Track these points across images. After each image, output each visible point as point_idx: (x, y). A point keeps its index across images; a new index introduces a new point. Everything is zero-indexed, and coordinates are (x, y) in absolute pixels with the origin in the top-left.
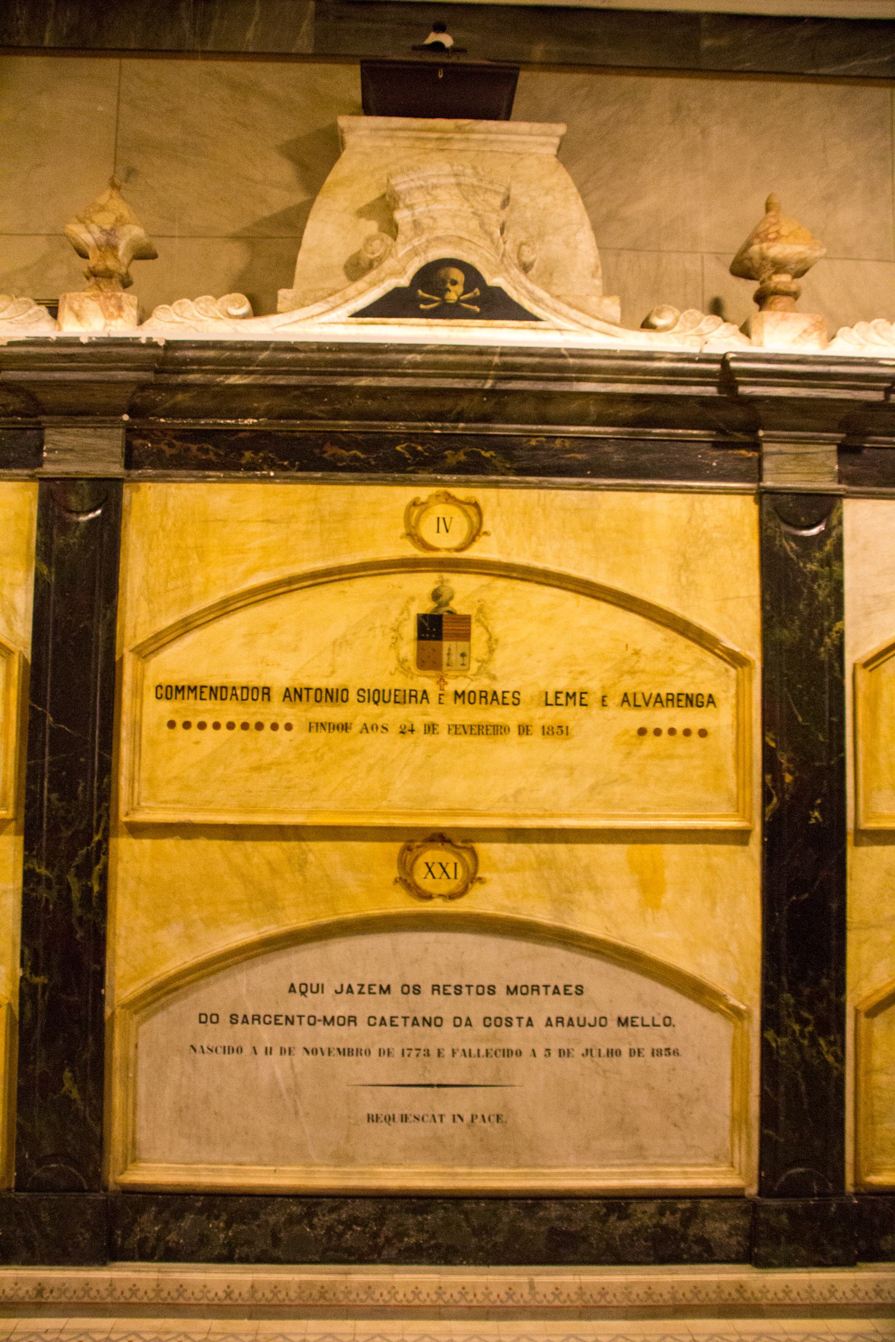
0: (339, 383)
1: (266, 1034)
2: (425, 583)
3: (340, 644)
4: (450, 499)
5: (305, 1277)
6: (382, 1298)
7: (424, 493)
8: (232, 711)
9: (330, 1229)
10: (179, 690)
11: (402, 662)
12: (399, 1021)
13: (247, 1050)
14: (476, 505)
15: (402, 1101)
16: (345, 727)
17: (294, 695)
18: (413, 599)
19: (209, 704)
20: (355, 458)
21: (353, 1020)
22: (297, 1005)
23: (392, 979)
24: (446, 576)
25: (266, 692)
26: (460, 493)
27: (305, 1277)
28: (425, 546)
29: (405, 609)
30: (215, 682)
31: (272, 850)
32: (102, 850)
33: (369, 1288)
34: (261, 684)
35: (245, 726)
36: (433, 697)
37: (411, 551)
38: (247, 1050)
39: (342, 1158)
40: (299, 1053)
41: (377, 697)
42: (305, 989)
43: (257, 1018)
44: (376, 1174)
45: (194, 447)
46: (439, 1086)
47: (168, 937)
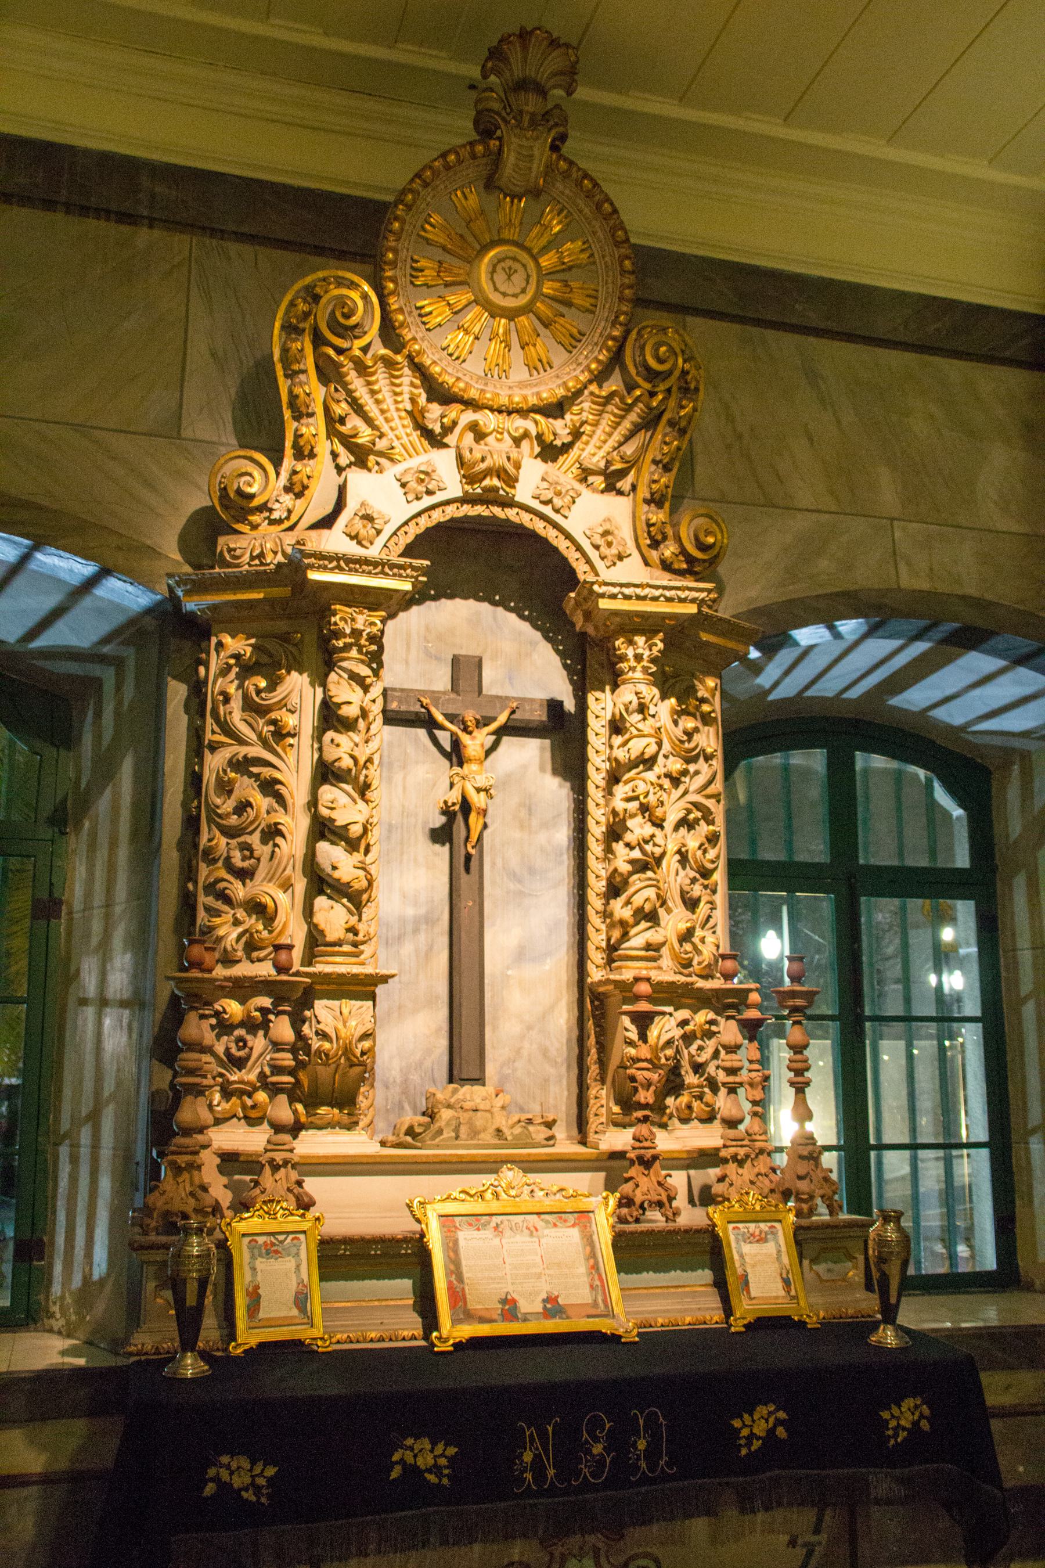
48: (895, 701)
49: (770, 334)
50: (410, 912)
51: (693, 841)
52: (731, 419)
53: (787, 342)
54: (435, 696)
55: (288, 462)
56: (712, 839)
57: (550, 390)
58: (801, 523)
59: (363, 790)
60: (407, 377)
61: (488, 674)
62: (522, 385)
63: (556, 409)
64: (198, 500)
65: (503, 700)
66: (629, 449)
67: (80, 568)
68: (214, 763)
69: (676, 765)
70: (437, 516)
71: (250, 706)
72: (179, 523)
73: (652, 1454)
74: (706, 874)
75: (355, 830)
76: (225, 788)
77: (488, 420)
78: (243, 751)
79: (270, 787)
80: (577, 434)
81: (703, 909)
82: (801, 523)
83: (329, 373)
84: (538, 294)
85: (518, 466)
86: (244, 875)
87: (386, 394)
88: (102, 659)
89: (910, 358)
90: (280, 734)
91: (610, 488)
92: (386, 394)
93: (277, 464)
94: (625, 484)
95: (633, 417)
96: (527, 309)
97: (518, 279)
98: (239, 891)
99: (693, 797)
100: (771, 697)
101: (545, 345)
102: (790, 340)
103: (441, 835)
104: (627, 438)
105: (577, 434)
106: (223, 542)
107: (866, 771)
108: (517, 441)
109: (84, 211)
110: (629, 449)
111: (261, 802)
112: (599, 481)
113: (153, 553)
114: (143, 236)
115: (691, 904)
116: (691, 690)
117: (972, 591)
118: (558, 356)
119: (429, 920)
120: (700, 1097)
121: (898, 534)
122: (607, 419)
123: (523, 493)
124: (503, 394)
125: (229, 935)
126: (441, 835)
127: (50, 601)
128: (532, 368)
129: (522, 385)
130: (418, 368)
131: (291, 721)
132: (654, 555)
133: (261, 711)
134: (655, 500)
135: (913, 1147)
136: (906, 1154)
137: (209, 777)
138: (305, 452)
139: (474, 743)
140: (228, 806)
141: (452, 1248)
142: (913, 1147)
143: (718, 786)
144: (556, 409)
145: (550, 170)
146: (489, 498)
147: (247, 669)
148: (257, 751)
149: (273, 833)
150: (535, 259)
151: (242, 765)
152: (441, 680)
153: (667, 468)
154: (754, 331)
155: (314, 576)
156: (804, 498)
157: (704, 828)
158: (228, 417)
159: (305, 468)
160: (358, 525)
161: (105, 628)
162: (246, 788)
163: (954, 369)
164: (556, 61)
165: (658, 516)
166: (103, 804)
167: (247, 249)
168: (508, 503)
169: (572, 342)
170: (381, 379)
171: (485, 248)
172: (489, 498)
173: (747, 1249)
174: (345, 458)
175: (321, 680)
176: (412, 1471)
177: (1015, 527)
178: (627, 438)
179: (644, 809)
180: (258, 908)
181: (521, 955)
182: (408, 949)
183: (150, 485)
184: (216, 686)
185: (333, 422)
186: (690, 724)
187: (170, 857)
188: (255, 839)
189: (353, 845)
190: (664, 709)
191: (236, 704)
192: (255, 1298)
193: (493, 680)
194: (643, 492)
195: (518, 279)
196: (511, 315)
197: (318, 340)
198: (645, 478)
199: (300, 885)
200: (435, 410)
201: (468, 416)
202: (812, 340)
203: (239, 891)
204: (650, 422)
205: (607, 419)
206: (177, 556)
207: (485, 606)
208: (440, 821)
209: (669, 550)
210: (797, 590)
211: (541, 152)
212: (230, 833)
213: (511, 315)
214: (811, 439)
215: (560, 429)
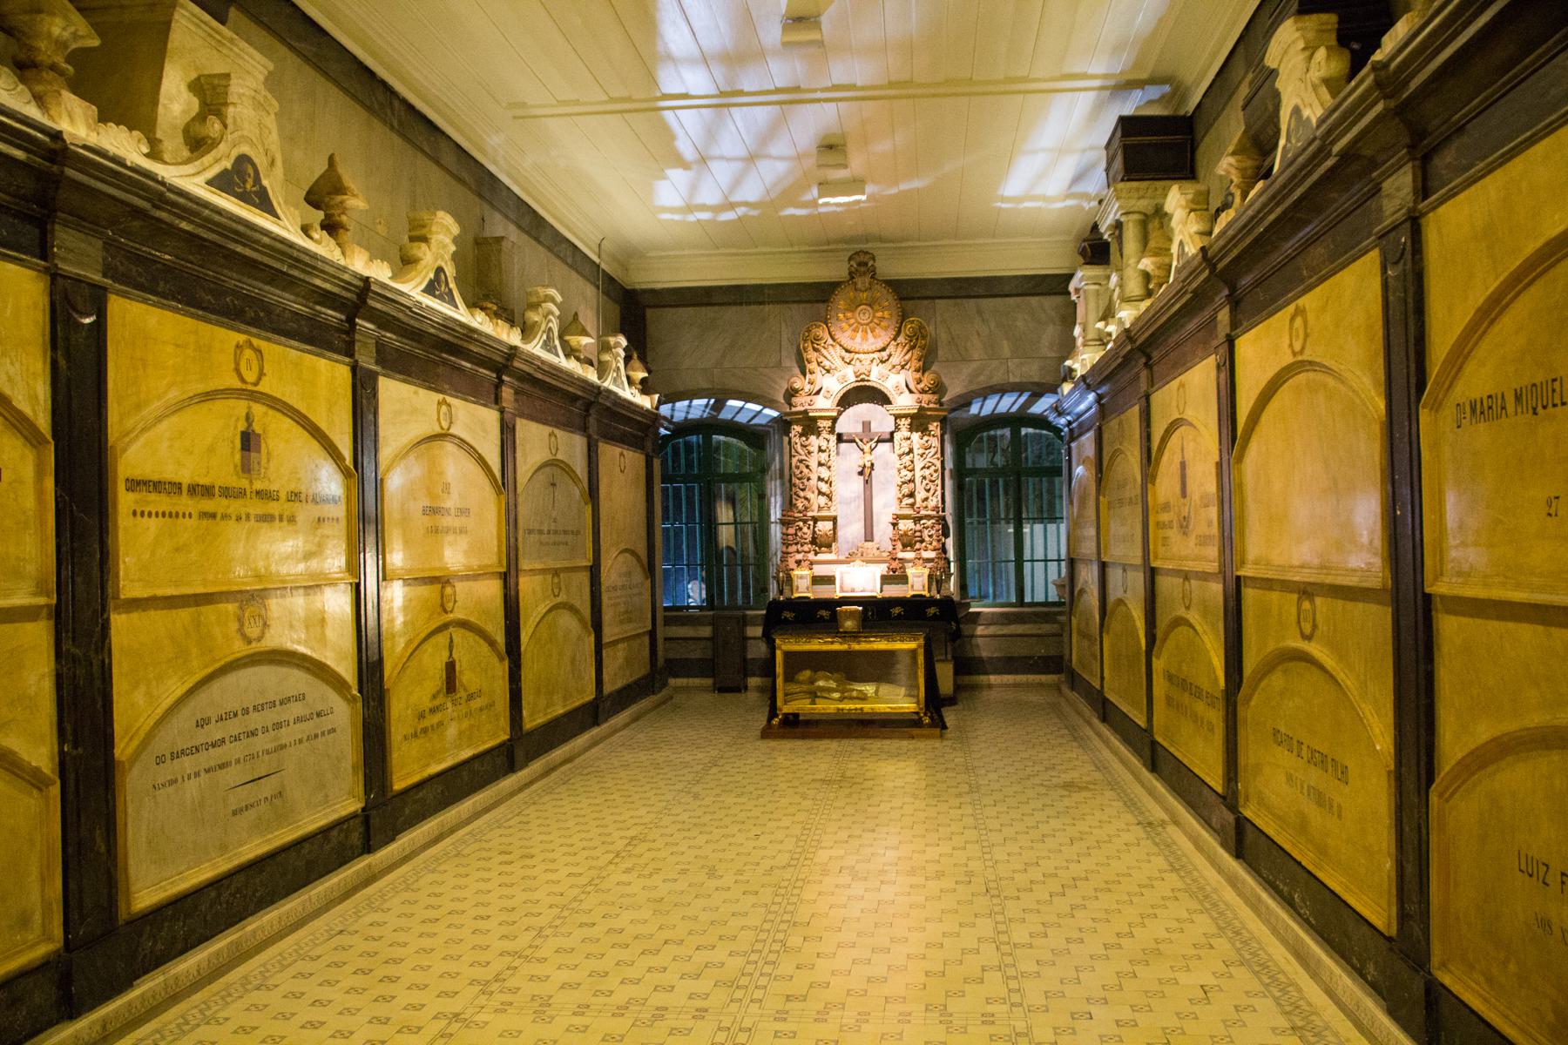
0: (229, 246)
1: (188, 763)
2: (240, 407)
3: (211, 450)
4: (251, 345)
5: (229, 940)
6: (260, 937)
7: (241, 338)
8: (162, 502)
9: (227, 902)
10: (138, 483)
11: (236, 466)
12: (242, 737)
13: (180, 780)
14: (260, 352)
15: (245, 795)
16: (213, 516)
17: (194, 490)
18: (238, 419)
19: (153, 496)
20: (209, 302)
21: (223, 741)
22: (201, 737)
23: (237, 707)
24: (251, 403)
25: (179, 486)
26: (256, 341)
27: (229, 940)
28: (243, 380)
29: (236, 427)
30: (155, 478)
31: (184, 615)
32: (106, 628)
33: (254, 931)
34: (177, 481)
35: (170, 515)
36: (248, 493)
37: (237, 384)
38: (180, 780)
39: (223, 848)
40: (202, 774)
41: (227, 492)
42: (202, 723)
43: (183, 752)
44: (240, 853)
45: (134, 269)
46: (260, 778)
47: (139, 697)
48: (1029, 411)
49: (964, 301)
50: (853, 495)
51: (927, 472)
52: (951, 333)
53: (971, 304)
54: (857, 435)
55: (808, 376)
56: (936, 471)
57: (880, 345)
58: (975, 365)
59: (829, 467)
60: (838, 347)
61: (872, 425)
62: (872, 344)
63: (883, 349)
64: (786, 386)
65: (877, 433)
66: (907, 357)
67: (758, 408)
68: (794, 461)
69: (921, 451)
70: (849, 387)
71: (802, 445)
72: (783, 391)
73: (872, 615)
74: (933, 481)
75: (826, 479)
76: (798, 467)
77: (862, 356)
78: (801, 457)
79: (807, 467)
80: (890, 356)
81: (932, 492)
82: (975, 365)
83: (815, 350)
84: (874, 317)
85: (870, 372)
86: (803, 490)
87: (833, 353)
88: (770, 427)
89: (1019, 299)
90: (809, 453)
91: (903, 367)
92: (833, 353)
93: (805, 376)
94: (907, 367)
95: (907, 348)
96: (871, 322)
97: (867, 315)
98: (802, 494)
99: (928, 460)
100: (982, 415)
101: (878, 331)
102: (972, 301)
103: (861, 473)
104: (906, 354)
105: (890, 356)
106: (794, 400)
107: (1026, 435)
108: (872, 361)
109: (750, 304)
110: (907, 357)
111: (806, 471)
112: (899, 367)
113: (777, 402)
114: (767, 308)
115: (928, 491)
116: (927, 429)
117: (1036, 380)
118: (883, 333)
119: (859, 497)
120: (931, 544)
121: (1010, 364)
122: (899, 349)
123: (872, 377)
124: (865, 347)
125: (800, 504)
126: (861, 473)
127: (753, 414)
128: (875, 337)
129: (872, 344)
130: (841, 345)
131: (811, 449)
132: (920, 386)
133: (805, 446)
134: (917, 371)
135: (1046, 561)
136: (1043, 563)
137: (793, 465)
138: (812, 373)
139: (867, 448)
140: (798, 472)
141: (842, 579)
142: (1046, 561)
143: (939, 455)
144: (883, 349)
145: (870, 284)
146: (863, 380)
147: (801, 435)
148: (804, 457)
149: (809, 479)
150: (870, 305)
151: (801, 461)
152: (859, 429)
153: (919, 360)
154: (959, 301)
155: (810, 414)
156: (976, 356)
157: (933, 468)
158: (793, 357)
159: (813, 377)
160: (826, 394)
161: (768, 420)
162: (802, 467)
163: (1034, 300)
164: (867, 257)
165: (918, 375)
166: (773, 468)
167: (795, 306)
168: (868, 381)
169: (886, 329)
170: (831, 348)
171: (857, 307)
172: (863, 380)
173: (915, 579)
174: (824, 372)
175: (818, 438)
176: (822, 617)
177: (1054, 355)
178: (906, 354)
179: (905, 467)
180: (806, 499)
181: (885, 506)
182: (853, 505)
183: (775, 382)
184: (793, 440)
185: (819, 364)
186: (926, 438)
187: (788, 484)
188: (805, 481)
189: (826, 482)
190: (916, 436)
191: (799, 445)
192: (798, 587)
193: (874, 427)
194: (913, 369)
195: (867, 315)
196: (867, 324)
197: (812, 343)
198: (913, 364)
199: (816, 492)
200: (848, 354)
201: (857, 356)
202: (981, 300)
203: (802, 494)
204: (912, 348)
205: (899, 349)
206: (783, 401)
207: (872, 405)
208: (860, 469)
209: (922, 385)
210: (973, 387)
211: (867, 279)
212: (799, 479)
213: (867, 324)
214: (979, 334)
215: (884, 355)
